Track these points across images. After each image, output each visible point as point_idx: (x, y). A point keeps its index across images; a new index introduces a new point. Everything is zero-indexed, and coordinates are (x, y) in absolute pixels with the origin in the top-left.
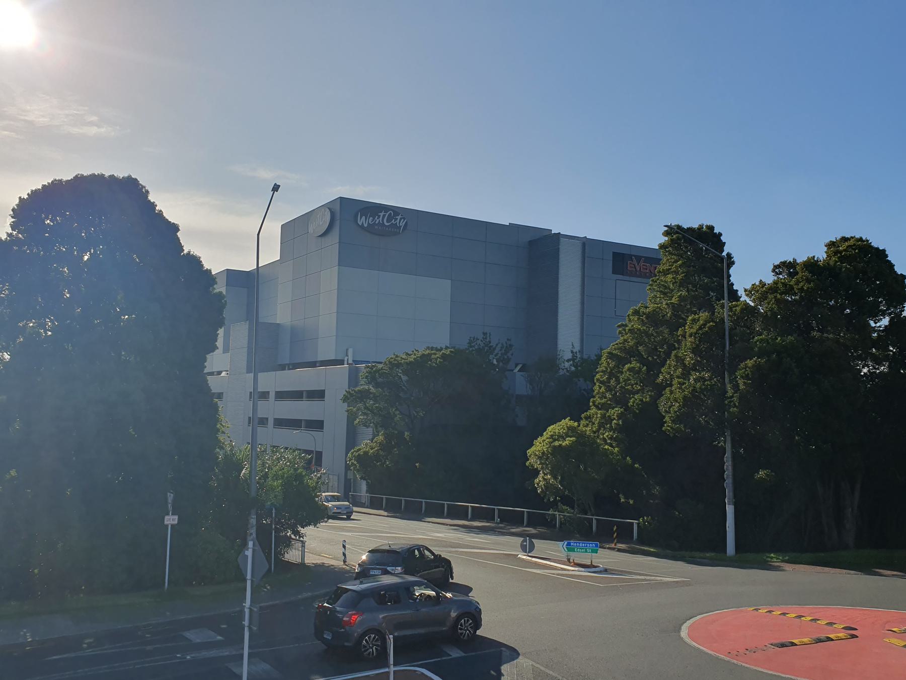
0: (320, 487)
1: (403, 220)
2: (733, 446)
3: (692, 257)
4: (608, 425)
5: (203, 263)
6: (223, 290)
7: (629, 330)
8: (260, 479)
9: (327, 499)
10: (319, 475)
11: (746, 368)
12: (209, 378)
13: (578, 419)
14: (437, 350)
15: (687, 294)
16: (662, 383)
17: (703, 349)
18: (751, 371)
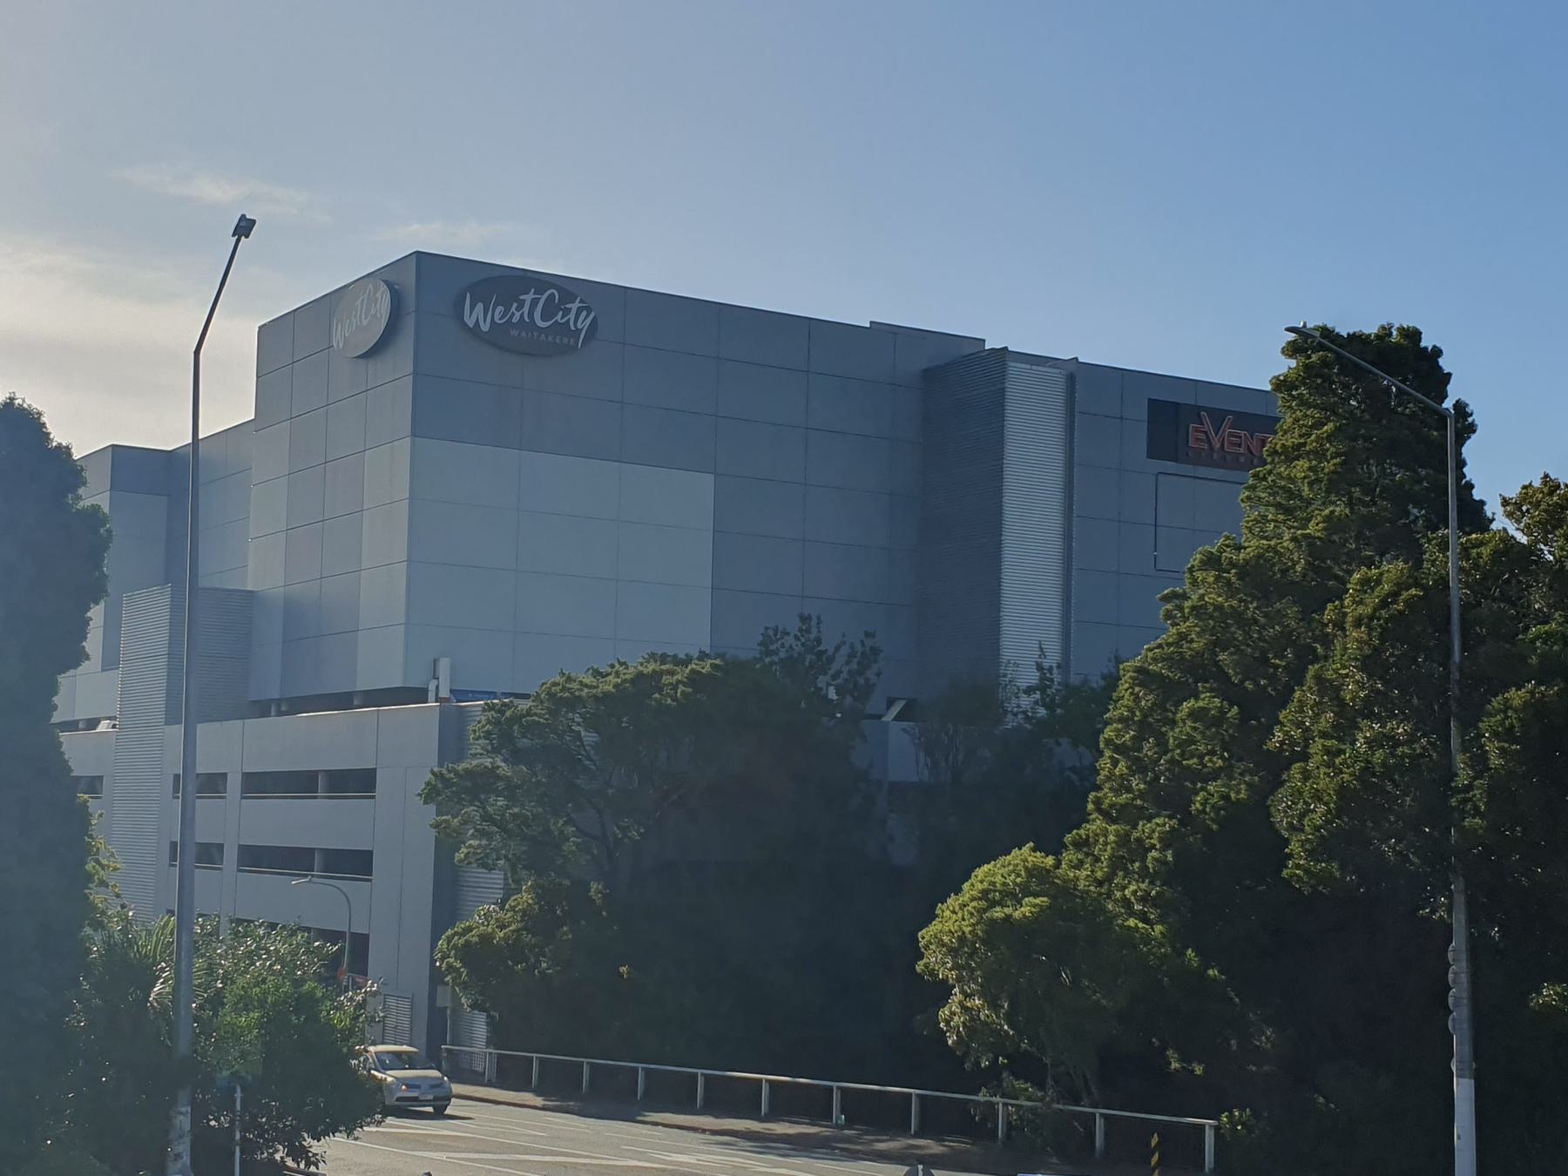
0: (362, 1031)
1: (584, 313)
2: (1472, 921)
3: (1363, 412)
4: (1137, 864)
5: (50, 428)
6: (103, 501)
7: (1193, 608)
8: (201, 1007)
9: (382, 1062)
10: (360, 998)
11: (1505, 712)
12: (64, 736)
13: (1056, 849)
14: (677, 661)
15: (1347, 511)
16: (1281, 750)
17: (1392, 660)
18: (1520, 719)
